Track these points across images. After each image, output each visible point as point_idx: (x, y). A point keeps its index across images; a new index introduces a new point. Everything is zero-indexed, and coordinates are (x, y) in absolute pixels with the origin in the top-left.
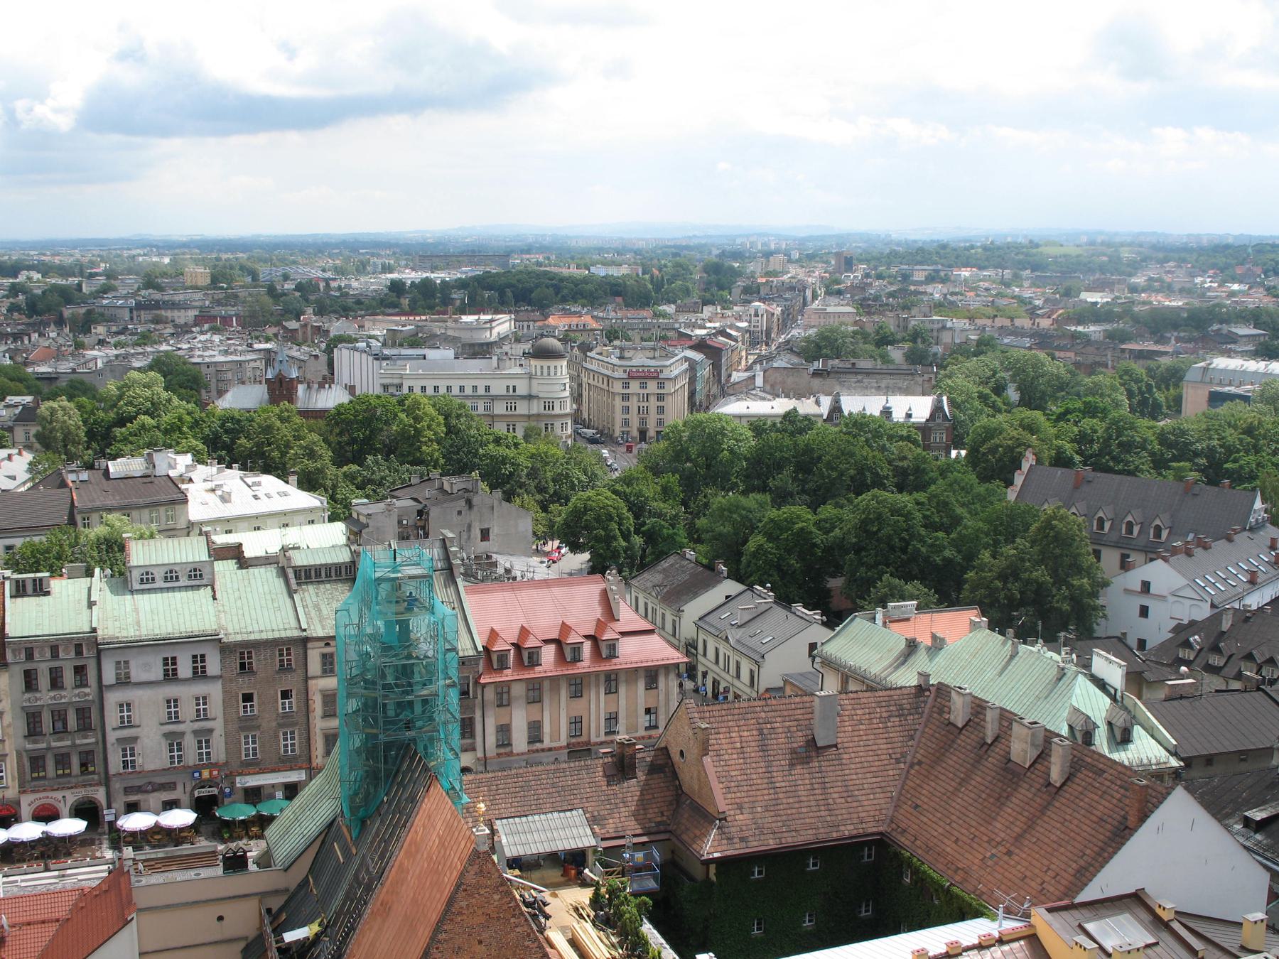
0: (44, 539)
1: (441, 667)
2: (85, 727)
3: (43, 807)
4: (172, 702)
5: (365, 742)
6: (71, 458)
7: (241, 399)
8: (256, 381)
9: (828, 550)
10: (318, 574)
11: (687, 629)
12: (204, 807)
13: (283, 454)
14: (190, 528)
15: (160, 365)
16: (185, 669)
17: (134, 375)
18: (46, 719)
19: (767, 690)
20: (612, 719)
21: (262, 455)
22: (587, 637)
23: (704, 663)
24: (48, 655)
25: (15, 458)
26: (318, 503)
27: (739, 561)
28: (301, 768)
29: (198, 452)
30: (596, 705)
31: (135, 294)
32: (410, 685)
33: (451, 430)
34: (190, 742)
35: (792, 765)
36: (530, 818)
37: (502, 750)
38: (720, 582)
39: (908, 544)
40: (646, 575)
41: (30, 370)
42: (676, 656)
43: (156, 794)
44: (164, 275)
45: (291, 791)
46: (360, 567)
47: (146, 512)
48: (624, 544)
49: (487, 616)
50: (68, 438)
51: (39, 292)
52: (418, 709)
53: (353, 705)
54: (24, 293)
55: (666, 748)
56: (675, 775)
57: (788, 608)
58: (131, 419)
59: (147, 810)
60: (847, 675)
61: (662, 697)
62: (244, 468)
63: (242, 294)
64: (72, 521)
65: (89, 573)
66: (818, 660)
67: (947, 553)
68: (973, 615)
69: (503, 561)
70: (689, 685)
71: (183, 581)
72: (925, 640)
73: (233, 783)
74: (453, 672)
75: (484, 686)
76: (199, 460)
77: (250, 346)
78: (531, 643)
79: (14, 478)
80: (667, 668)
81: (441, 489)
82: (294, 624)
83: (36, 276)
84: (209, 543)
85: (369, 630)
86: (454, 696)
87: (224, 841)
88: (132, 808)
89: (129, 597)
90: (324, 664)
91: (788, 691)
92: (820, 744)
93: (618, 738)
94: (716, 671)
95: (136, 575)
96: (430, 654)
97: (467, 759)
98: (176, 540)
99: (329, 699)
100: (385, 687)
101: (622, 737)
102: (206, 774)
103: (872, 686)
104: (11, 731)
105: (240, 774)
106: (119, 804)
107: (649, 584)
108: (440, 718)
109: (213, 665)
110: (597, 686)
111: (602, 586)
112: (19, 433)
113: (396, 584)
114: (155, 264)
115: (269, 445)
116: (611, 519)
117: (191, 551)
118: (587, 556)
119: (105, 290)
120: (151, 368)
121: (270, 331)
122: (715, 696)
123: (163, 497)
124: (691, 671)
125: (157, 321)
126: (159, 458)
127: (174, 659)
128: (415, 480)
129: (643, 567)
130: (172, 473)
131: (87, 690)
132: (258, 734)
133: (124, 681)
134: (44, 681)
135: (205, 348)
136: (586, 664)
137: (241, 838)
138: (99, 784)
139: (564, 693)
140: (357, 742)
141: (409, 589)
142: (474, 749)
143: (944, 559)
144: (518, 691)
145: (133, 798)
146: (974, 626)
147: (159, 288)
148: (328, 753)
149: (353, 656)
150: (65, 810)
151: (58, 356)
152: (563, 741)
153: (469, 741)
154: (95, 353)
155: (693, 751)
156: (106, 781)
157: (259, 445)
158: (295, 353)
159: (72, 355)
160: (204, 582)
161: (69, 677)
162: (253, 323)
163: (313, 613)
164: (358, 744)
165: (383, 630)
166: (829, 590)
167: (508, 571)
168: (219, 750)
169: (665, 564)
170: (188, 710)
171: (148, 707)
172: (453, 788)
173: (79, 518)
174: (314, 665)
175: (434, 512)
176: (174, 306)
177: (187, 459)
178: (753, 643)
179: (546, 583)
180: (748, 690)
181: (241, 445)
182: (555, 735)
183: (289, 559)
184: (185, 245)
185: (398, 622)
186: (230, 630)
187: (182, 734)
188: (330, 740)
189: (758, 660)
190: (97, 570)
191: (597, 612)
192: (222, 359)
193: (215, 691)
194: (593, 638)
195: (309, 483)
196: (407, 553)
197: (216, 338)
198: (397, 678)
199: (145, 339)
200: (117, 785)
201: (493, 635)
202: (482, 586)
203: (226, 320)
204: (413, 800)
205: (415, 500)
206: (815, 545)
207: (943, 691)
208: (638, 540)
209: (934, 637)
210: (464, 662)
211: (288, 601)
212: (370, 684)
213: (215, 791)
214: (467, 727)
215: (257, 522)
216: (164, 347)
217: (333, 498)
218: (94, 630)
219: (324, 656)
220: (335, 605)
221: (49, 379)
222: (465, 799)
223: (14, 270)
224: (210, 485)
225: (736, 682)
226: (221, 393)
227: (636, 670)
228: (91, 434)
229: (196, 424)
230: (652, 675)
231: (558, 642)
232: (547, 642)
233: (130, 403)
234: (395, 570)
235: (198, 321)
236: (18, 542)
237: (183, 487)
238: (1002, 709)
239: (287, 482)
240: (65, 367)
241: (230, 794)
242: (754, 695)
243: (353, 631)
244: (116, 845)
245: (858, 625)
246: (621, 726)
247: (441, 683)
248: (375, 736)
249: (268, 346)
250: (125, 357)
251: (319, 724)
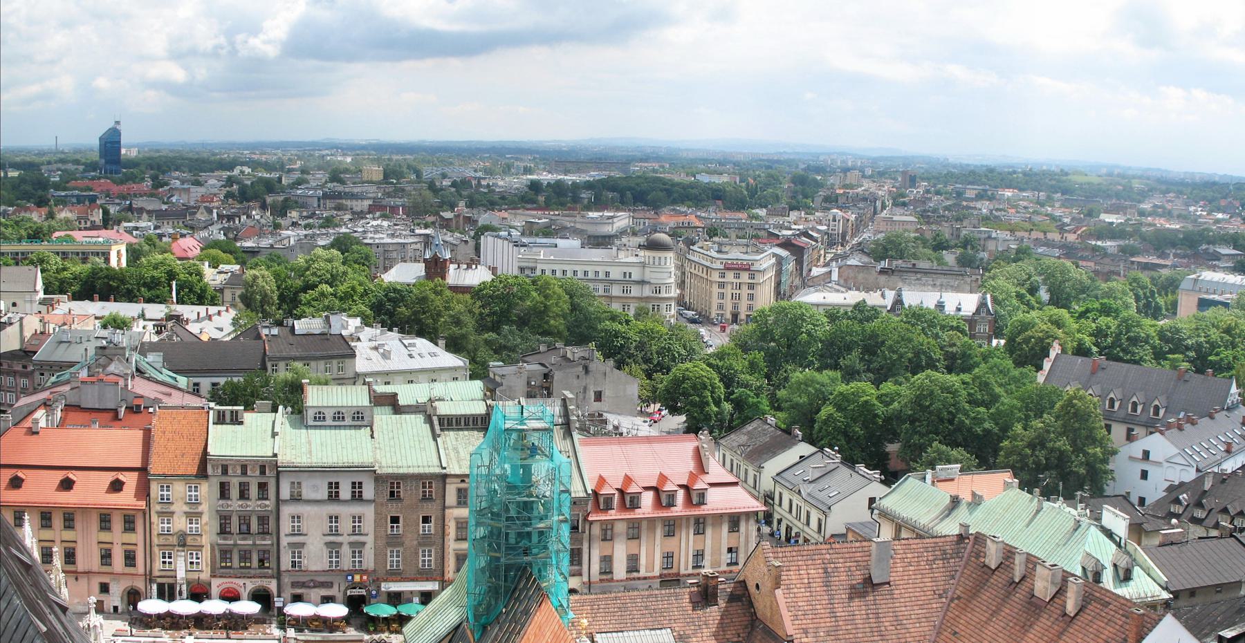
0: (242, 379)
1: (556, 505)
2: (264, 533)
3: (228, 590)
4: (334, 518)
5: (489, 564)
6: (266, 315)
7: (405, 274)
8: (416, 261)
9: (888, 420)
10: (458, 423)
11: (766, 484)
12: (355, 604)
13: (436, 321)
14: (356, 378)
15: (342, 244)
16: (345, 493)
17: (319, 251)
18: (235, 521)
19: (832, 536)
20: (699, 555)
21: (419, 321)
22: (681, 486)
23: (780, 512)
24: (239, 471)
25: (223, 313)
26: (461, 364)
27: (812, 427)
28: (435, 580)
29: (367, 317)
30: (686, 544)
31: (323, 186)
32: (530, 519)
33: (574, 308)
34: (346, 551)
35: (851, 598)
36: (625, 634)
37: (604, 577)
38: (795, 444)
39: (954, 416)
40: (732, 436)
41: (238, 244)
42: (757, 506)
43: (316, 590)
44: (346, 171)
45: (426, 597)
46: (493, 418)
47: (322, 363)
48: (716, 409)
49: (597, 464)
50: (265, 298)
51: (249, 183)
52: (535, 538)
53: (481, 532)
54: (238, 183)
55: (744, 581)
56: (751, 604)
57: (853, 469)
58: (313, 287)
59: (309, 602)
60: (900, 525)
61: (742, 539)
62: (402, 331)
63: (408, 188)
64: (264, 368)
65: (275, 410)
66: (876, 512)
67: (987, 425)
68: (1006, 476)
69: (613, 419)
70: (766, 529)
71: (348, 421)
72: (966, 497)
73: (379, 587)
74: (566, 510)
75: (591, 523)
76: (367, 322)
77: (413, 231)
78: (633, 489)
79: (221, 330)
80: (748, 515)
81: (564, 357)
82: (436, 462)
83: (247, 170)
84: (371, 391)
85: (498, 471)
86: (565, 530)
87: (369, 632)
88: (297, 598)
89: (304, 431)
90: (459, 497)
91: (850, 537)
92: (875, 581)
93: (703, 571)
94: (789, 519)
95: (311, 413)
96: (547, 494)
97: (574, 583)
98: (344, 388)
99: (462, 525)
100: (508, 519)
101: (707, 570)
102: (357, 578)
103: (920, 534)
104: (207, 528)
105: (385, 581)
106: (287, 594)
107: (735, 444)
108: (553, 547)
109: (368, 491)
110: (688, 527)
111: (696, 444)
112: (228, 295)
113: (522, 434)
114: (340, 162)
115: (424, 313)
116: (705, 387)
117: (356, 397)
118: (683, 418)
119: (299, 183)
120: (332, 246)
121: (430, 219)
122: (788, 539)
123: (336, 352)
124: (768, 518)
125: (339, 208)
126: (333, 319)
127: (337, 483)
128: (543, 348)
129: (731, 429)
130: (344, 333)
131: (267, 502)
132: (401, 549)
133: (296, 499)
134: (234, 492)
135: (376, 232)
136: (679, 509)
137: (383, 632)
138: (272, 577)
139: (659, 532)
140: (482, 562)
141: (534, 439)
142: (581, 575)
143: (985, 430)
144: (620, 528)
145: (299, 591)
146: (1007, 486)
147: (342, 182)
148: (458, 570)
149: (483, 491)
150: (245, 594)
151: (261, 234)
152: (657, 572)
153: (576, 568)
154: (289, 232)
155: (767, 584)
156: (278, 576)
157: (415, 313)
158: (448, 238)
159: (271, 233)
160: (365, 423)
161: (254, 491)
162: (416, 212)
163: (452, 454)
164: (483, 564)
165: (509, 472)
166: (888, 454)
167: (616, 428)
168: (369, 561)
169: (749, 428)
170: (346, 526)
171: (314, 520)
172: (561, 605)
173: (269, 365)
174: (451, 498)
175: (557, 375)
176: (353, 196)
177: (357, 321)
178: (821, 496)
179: (648, 440)
180: (816, 536)
181: (401, 313)
182: (650, 567)
183: (435, 409)
184: (363, 147)
185: (522, 466)
186: (384, 464)
187: (341, 544)
188: (461, 559)
189: (826, 511)
190: (281, 408)
191: (691, 466)
192: (389, 241)
193: (368, 512)
194: (686, 488)
195: (454, 346)
196: (532, 409)
197: (385, 224)
198: (519, 513)
199: (328, 223)
200: (286, 580)
201: (602, 481)
202: (593, 439)
203: (394, 210)
204: (527, 613)
205: (542, 365)
206: (877, 415)
207: (980, 539)
208: (727, 407)
209: (974, 494)
210: (575, 502)
211: (433, 443)
212: (496, 516)
213: (363, 592)
214: (576, 556)
215: (410, 376)
216: (343, 230)
217: (473, 360)
218: (275, 455)
219: (459, 490)
220: (472, 449)
221: (253, 252)
222: (571, 615)
223: (230, 166)
224: (374, 344)
225: (806, 529)
226: (386, 269)
227: (721, 515)
228: (282, 298)
229: (366, 293)
230: (734, 521)
231: (656, 490)
232: (647, 489)
233: (314, 274)
234: (522, 423)
235: (371, 210)
236: (222, 381)
237: (353, 344)
238: (1028, 554)
239: (437, 344)
240: (265, 243)
241: (376, 596)
242: (821, 540)
243: (484, 471)
244: (282, 626)
245: (910, 483)
246: (707, 562)
247: (556, 518)
248: (498, 559)
249: (428, 231)
250: (313, 236)
251: (452, 546)
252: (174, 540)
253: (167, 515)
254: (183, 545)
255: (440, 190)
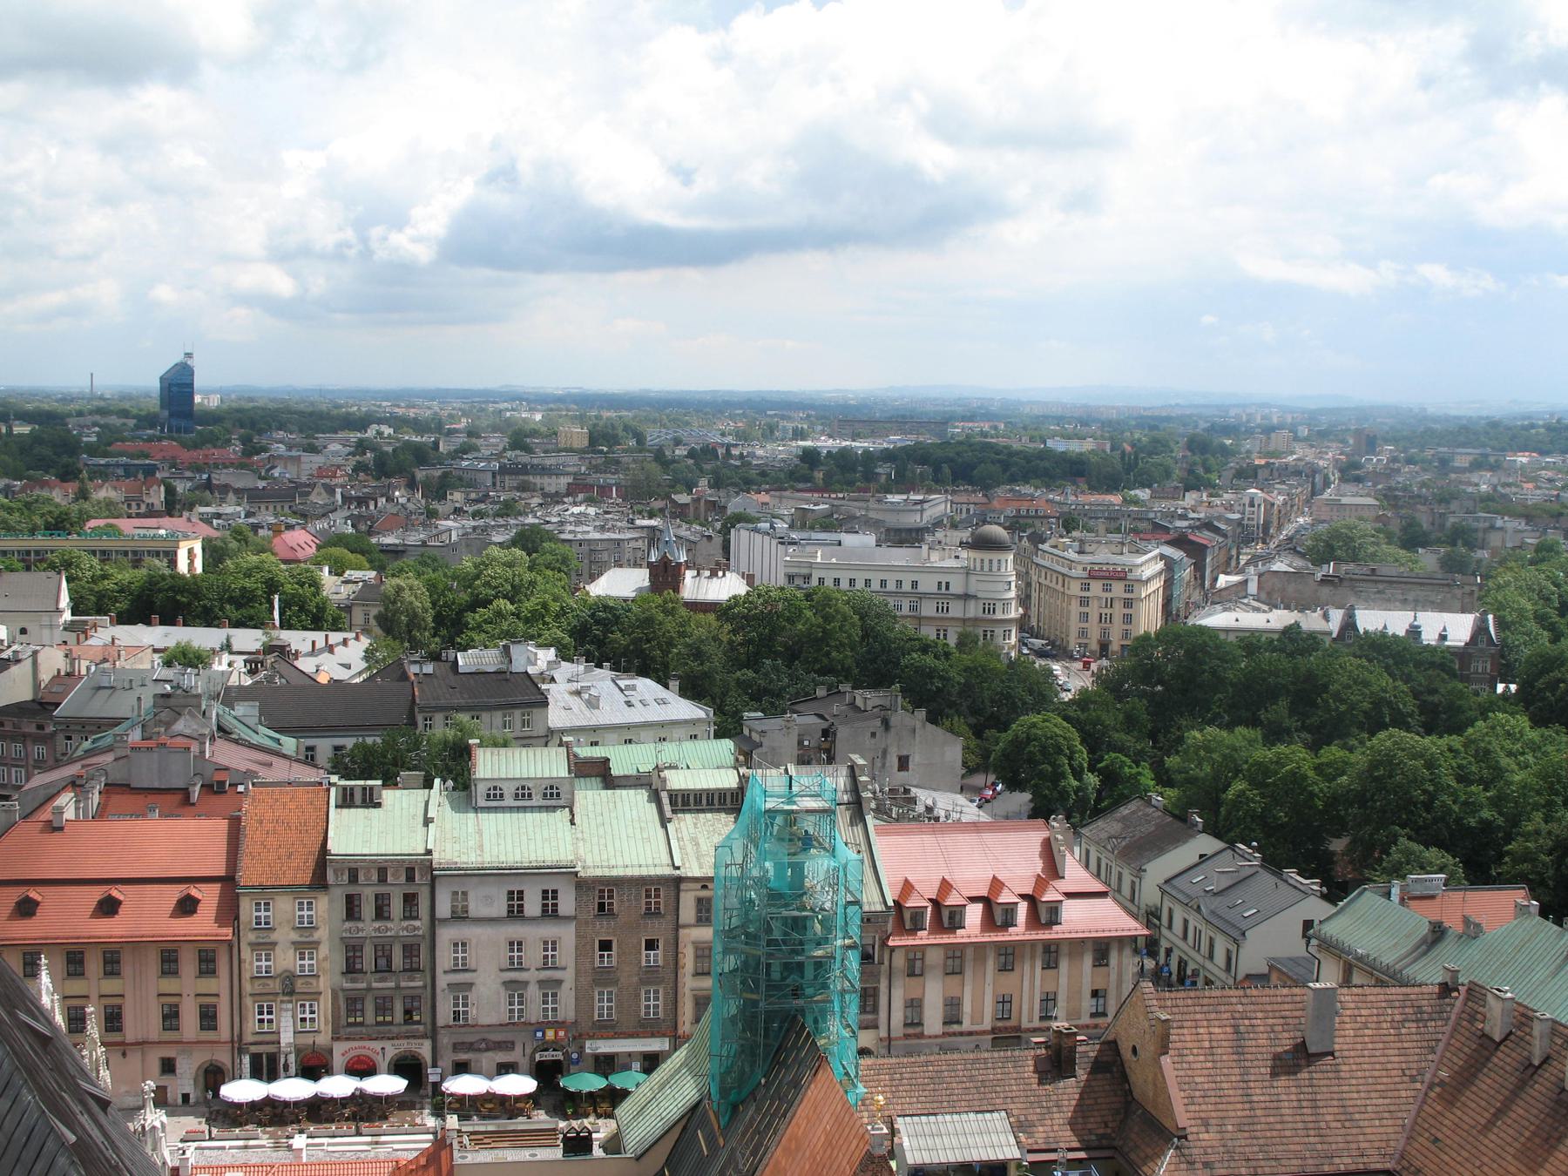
0: (379, 740)
1: (840, 922)
2: (412, 970)
3: (358, 1059)
4: (516, 945)
5: (742, 1011)
6: (415, 645)
7: (620, 584)
8: (636, 565)
9: (1334, 801)
10: (698, 800)
11: (1150, 894)
12: (547, 1073)
13: (666, 653)
14: (549, 737)
15: (529, 540)
16: (533, 906)
17: (495, 551)
18: (368, 952)
19: (1248, 976)
20: (1049, 1000)
21: (641, 654)
22: (1023, 896)
23: (1169, 938)
24: (375, 878)
25: (352, 643)
26: (702, 714)
27: (1217, 813)
28: (664, 1035)
29: (565, 646)
30: (1030, 982)
31: (499, 456)
32: (801, 943)
33: (867, 633)
34: (533, 992)
35: (1274, 1074)
36: (940, 1117)
37: (911, 1031)
38: (1192, 836)
39: (1432, 797)
40: (1100, 823)
41: (374, 540)
42: (1130, 926)
43: (490, 1054)
44: (534, 433)
45: (651, 1062)
46: (748, 794)
47: (499, 714)
48: (1075, 783)
50: (414, 621)
51: (390, 449)
52: (809, 972)
53: (731, 962)
54: (373, 450)
55: (1115, 1042)
56: (1124, 1078)
57: (1279, 875)
58: (486, 603)
59: (478, 1072)
60: (1352, 966)
61: (1113, 977)
62: (616, 668)
63: (626, 459)
64: (414, 724)
65: (428, 785)
66: (1314, 942)
67: (1486, 814)
68: (1519, 896)
69: (924, 797)
70: (1149, 964)
71: (537, 800)
72: (1454, 924)
73: (582, 1047)
74: (854, 930)
75: (893, 949)
76: (564, 655)
77: (632, 521)
78: (953, 900)
79: (348, 667)
80: (1121, 940)
81: (852, 704)
82: (666, 859)
83: (387, 431)
84: (571, 756)
85: (755, 873)
86: (853, 960)
87: (566, 1117)
88: (461, 1068)
89: (472, 815)
90: (699, 911)
91: (1274, 977)
92: (1312, 1049)
93: (1055, 1025)
94: (1183, 948)
95: (481, 789)
96: (827, 906)
97: (867, 1039)
98: (531, 751)
99: (703, 952)
100: (770, 943)
101: (1060, 1024)
102: (550, 1034)
103: (1385, 977)
104: (327, 965)
105: (592, 1037)
106: (447, 1060)
107: (1104, 835)
108: (836, 985)
109: (567, 904)
110: (1033, 958)
111: (1046, 834)
112: (358, 616)
113: (791, 818)
114: (524, 420)
115: (648, 641)
116: (1059, 751)
117: (549, 764)
118: (1027, 796)
119: (464, 450)
120: (514, 543)
121: (657, 504)
122: (1182, 980)
123: (519, 699)
124: (1151, 946)
125: (523, 487)
126: (515, 650)
127: (521, 893)
128: (821, 692)
129: (1097, 813)
130: (531, 670)
131: (417, 923)
132: (614, 989)
133: (460, 916)
134: (368, 909)
135: (578, 523)
136: (1019, 931)
137: (587, 1116)
138: (424, 1036)
139: (991, 964)
140: (733, 1009)
141: (809, 825)
142: (876, 1027)
143: (1482, 821)
144: (934, 957)
145: (463, 1057)
146: (1522, 910)
147: (528, 449)
148: (697, 1020)
149: (734, 901)
150: (383, 1064)
151: (407, 526)
152: (987, 1024)
153: (870, 1017)
154: (450, 523)
155: (1148, 1049)
156: (433, 1034)
157: (636, 641)
158: (683, 532)
159: (423, 524)
160: (561, 802)
161: (397, 906)
162: (638, 495)
163: (689, 848)
164: (733, 1011)
165: (771, 873)
166: (1333, 853)
167: (929, 809)
168: (567, 1007)
169: (1124, 811)
170: (532, 956)
172: (847, 1074)
173: (420, 719)
174: (688, 912)
175: (843, 732)
176: (544, 471)
177: (551, 653)
178: (1231, 915)
179: (976, 827)
180: (1223, 975)
181: (615, 641)
182: (977, 1016)
183: (664, 780)
184: (560, 399)
185: (790, 865)
186: (589, 863)
187: (526, 983)
188: (701, 1003)
189: (1238, 937)
190: (437, 781)
191: (1038, 866)
192: (597, 536)
193: (566, 935)
194: (1031, 899)
195: (692, 690)
196: (805, 781)
197: (592, 511)
198: (786, 934)
199: (508, 509)
200: (445, 1040)
201: (907, 887)
202: (896, 826)
203: (604, 491)
204: (796, 1085)
205: (821, 716)
206: (1312, 795)
207: (1476, 993)
208: (1092, 780)
209: (1466, 921)
210: (868, 919)
211: (661, 832)
212: (752, 938)
213: (559, 1056)
214: (869, 999)
215: (629, 733)
216: (530, 520)
217: (719, 710)
218: (429, 852)
219: (699, 901)
220: (717, 839)
221: (396, 552)
222: (861, 1089)
223: (361, 423)
224: (576, 686)
225: (1208, 964)
226: (593, 578)
227: (1083, 940)
228: (439, 619)
229: (563, 612)
230: (1101, 949)
231: (987, 902)
232: (973, 899)
233: (487, 584)
234: (790, 801)
235: (571, 491)
236: (349, 742)
237: (544, 687)
238: (1554, 1021)
239: (666, 686)
240: (414, 538)
241: (578, 1062)
242: (1231, 982)
243: (735, 872)
244: (438, 1112)
245: (1367, 901)
246: (1060, 1010)
247: (839, 942)
248: (755, 1003)
249: (653, 522)
250: (485, 529)
251: (689, 984)
252: (275, 986)
253: (265, 947)
254: (290, 991)
255: (672, 465)
